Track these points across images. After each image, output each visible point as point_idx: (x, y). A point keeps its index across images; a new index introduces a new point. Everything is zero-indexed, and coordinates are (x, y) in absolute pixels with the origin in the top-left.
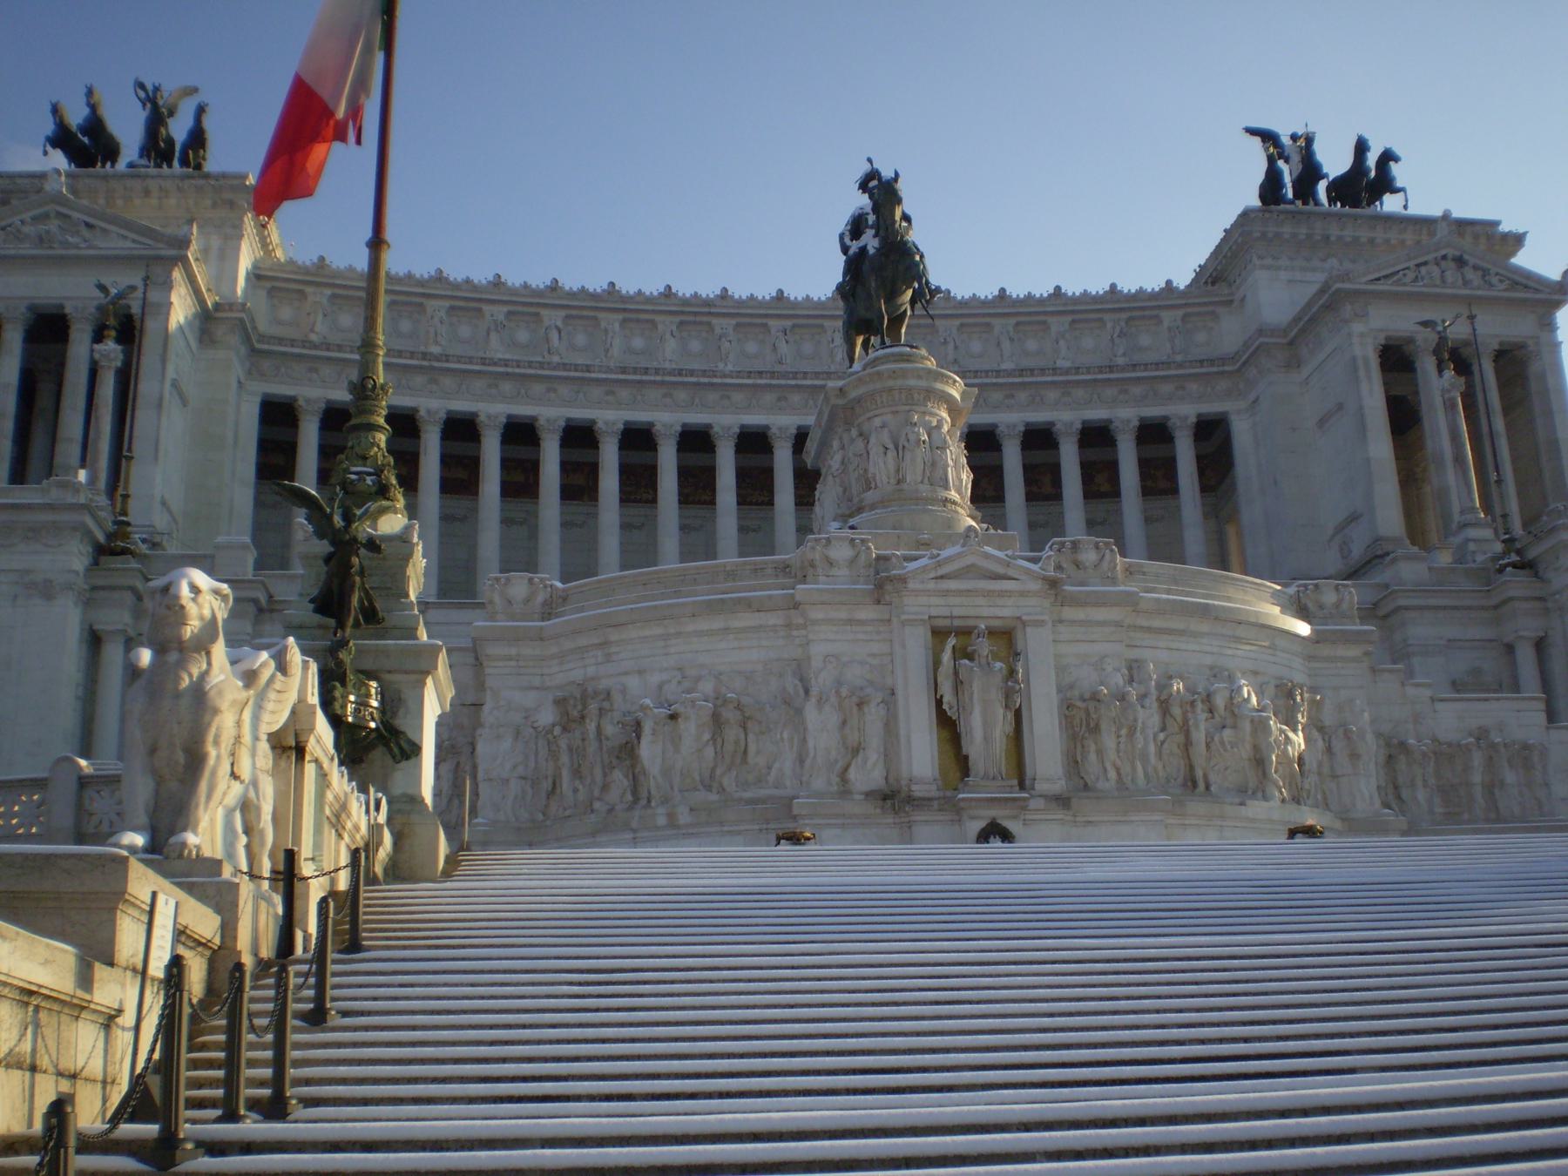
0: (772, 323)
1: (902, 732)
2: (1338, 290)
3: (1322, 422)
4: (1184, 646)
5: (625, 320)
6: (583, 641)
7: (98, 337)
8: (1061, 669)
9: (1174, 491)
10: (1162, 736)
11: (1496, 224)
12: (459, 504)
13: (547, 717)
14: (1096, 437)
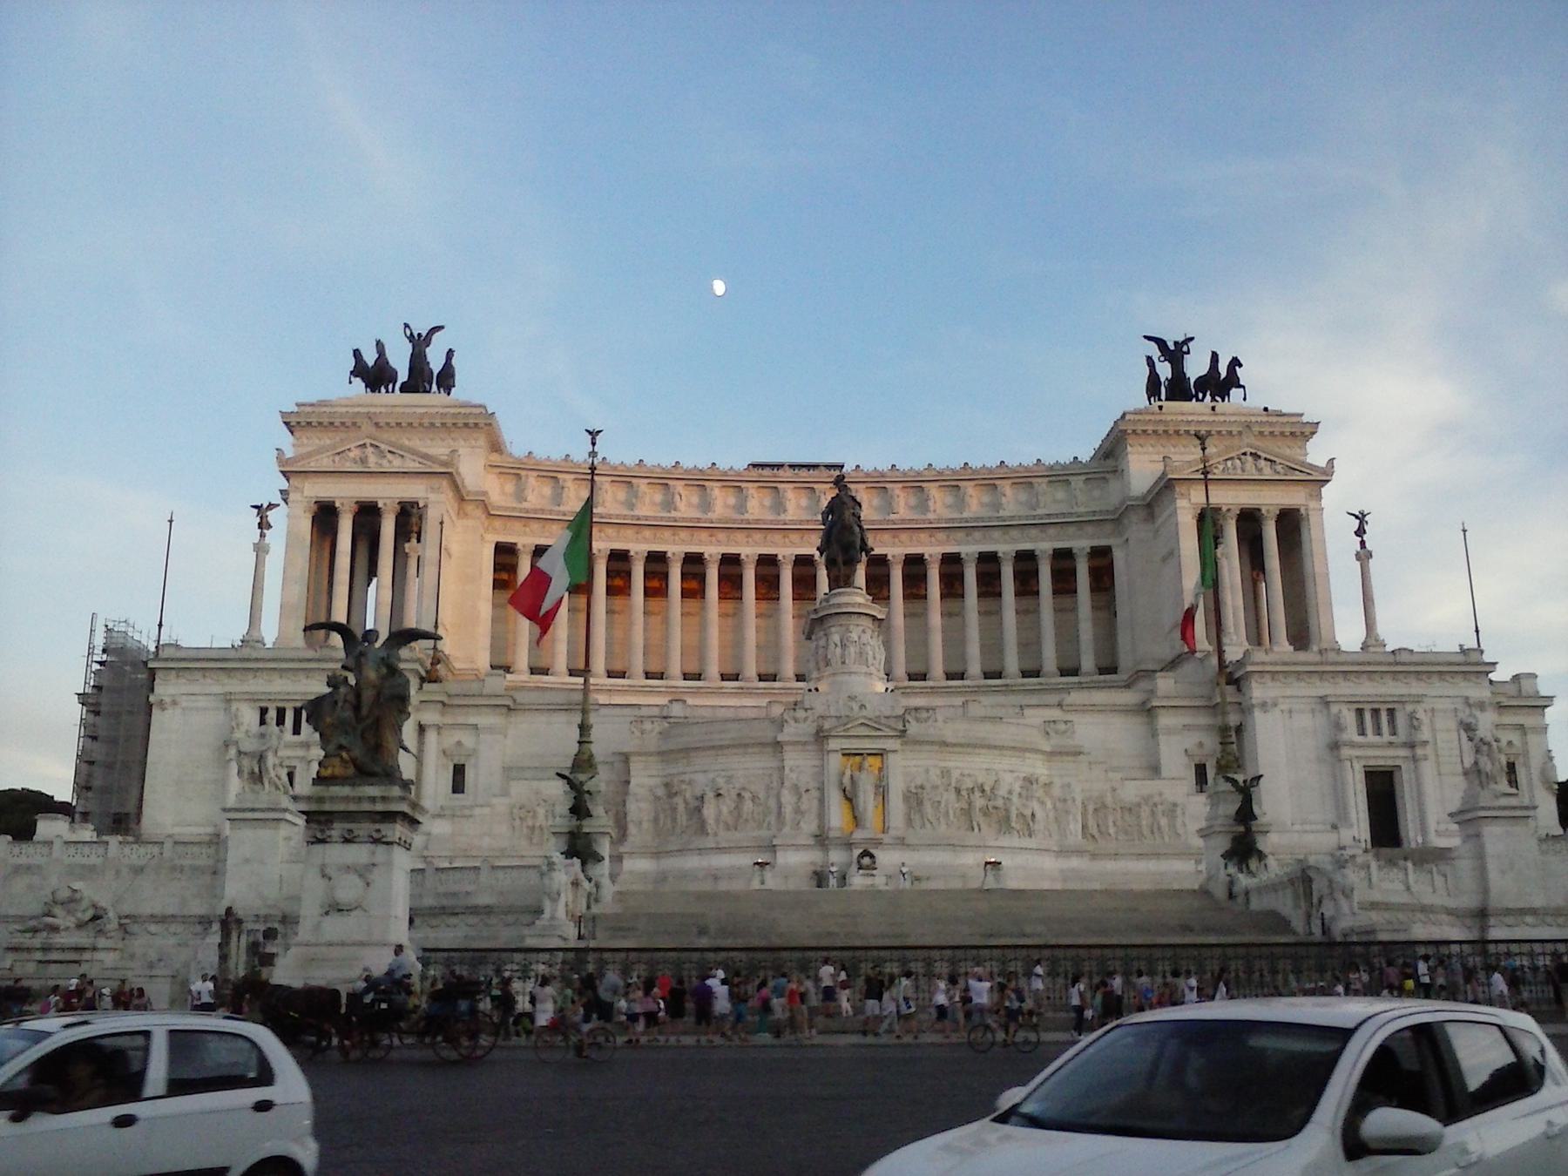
3: (1164, 559)
13: (661, 792)
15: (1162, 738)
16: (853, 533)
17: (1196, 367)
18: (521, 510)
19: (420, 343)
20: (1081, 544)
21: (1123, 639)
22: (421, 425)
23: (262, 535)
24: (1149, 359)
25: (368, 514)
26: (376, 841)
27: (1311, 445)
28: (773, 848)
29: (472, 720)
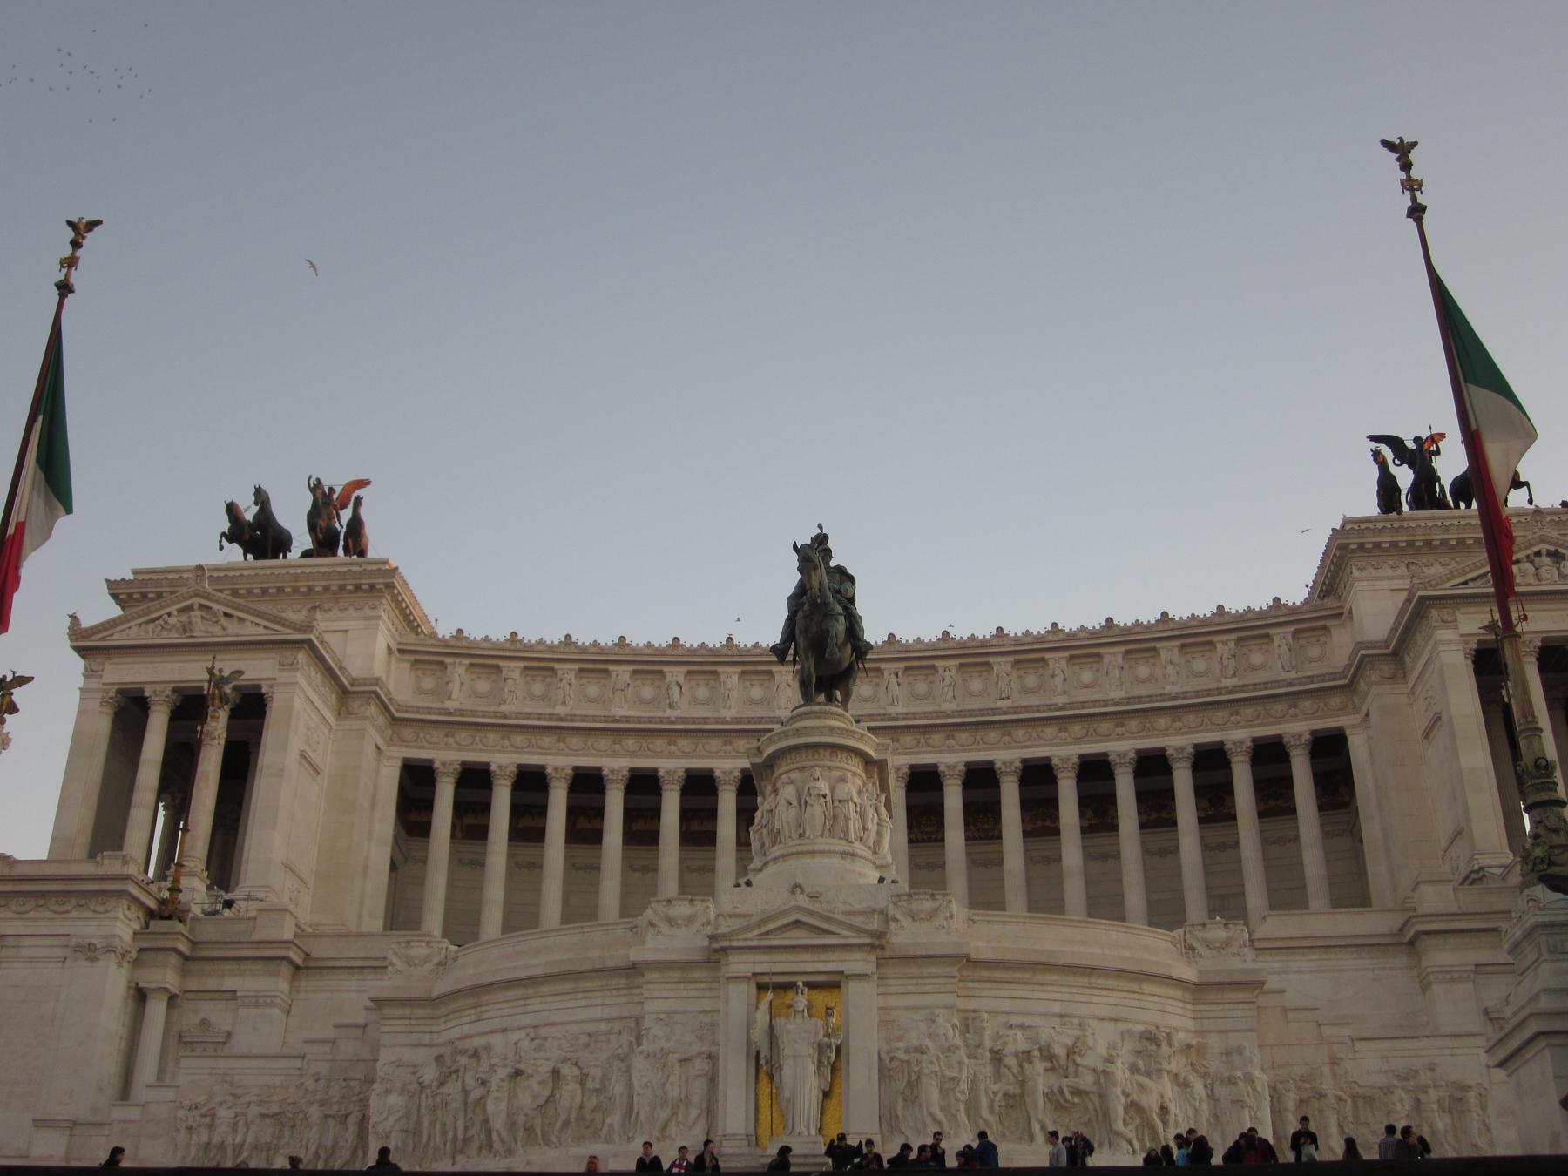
0: (883, 666)
1: (721, 1086)
2: (1421, 597)
3: (1427, 734)
4: (1028, 995)
5: (744, 673)
6: (462, 1003)
7: (234, 715)
8: (884, 1024)
9: (1294, 811)
10: (995, 1087)
12: (584, 852)
13: (430, 1074)
14: (1211, 761)
15: (1438, 989)
16: (829, 615)
18: (440, 712)
21: (1377, 870)
22: (296, 590)
25: (189, 707)
29: (229, 984)
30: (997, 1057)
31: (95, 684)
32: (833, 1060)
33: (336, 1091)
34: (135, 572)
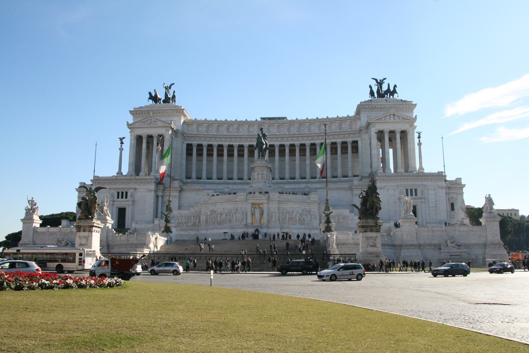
8: (268, 208)
11: (412, 102)
13: (209, 213)
17: (385, 88)
19: (168, 88)
20: (349, 140)
23: (121, 146)
24: (370, 87)
26: (89, 231)
27: (414, 111)
28: (234, 228)
30: (282, 213)
31: (133, 134)
32: (262, 214)
33: (195, 215)
34: (134, 108)
